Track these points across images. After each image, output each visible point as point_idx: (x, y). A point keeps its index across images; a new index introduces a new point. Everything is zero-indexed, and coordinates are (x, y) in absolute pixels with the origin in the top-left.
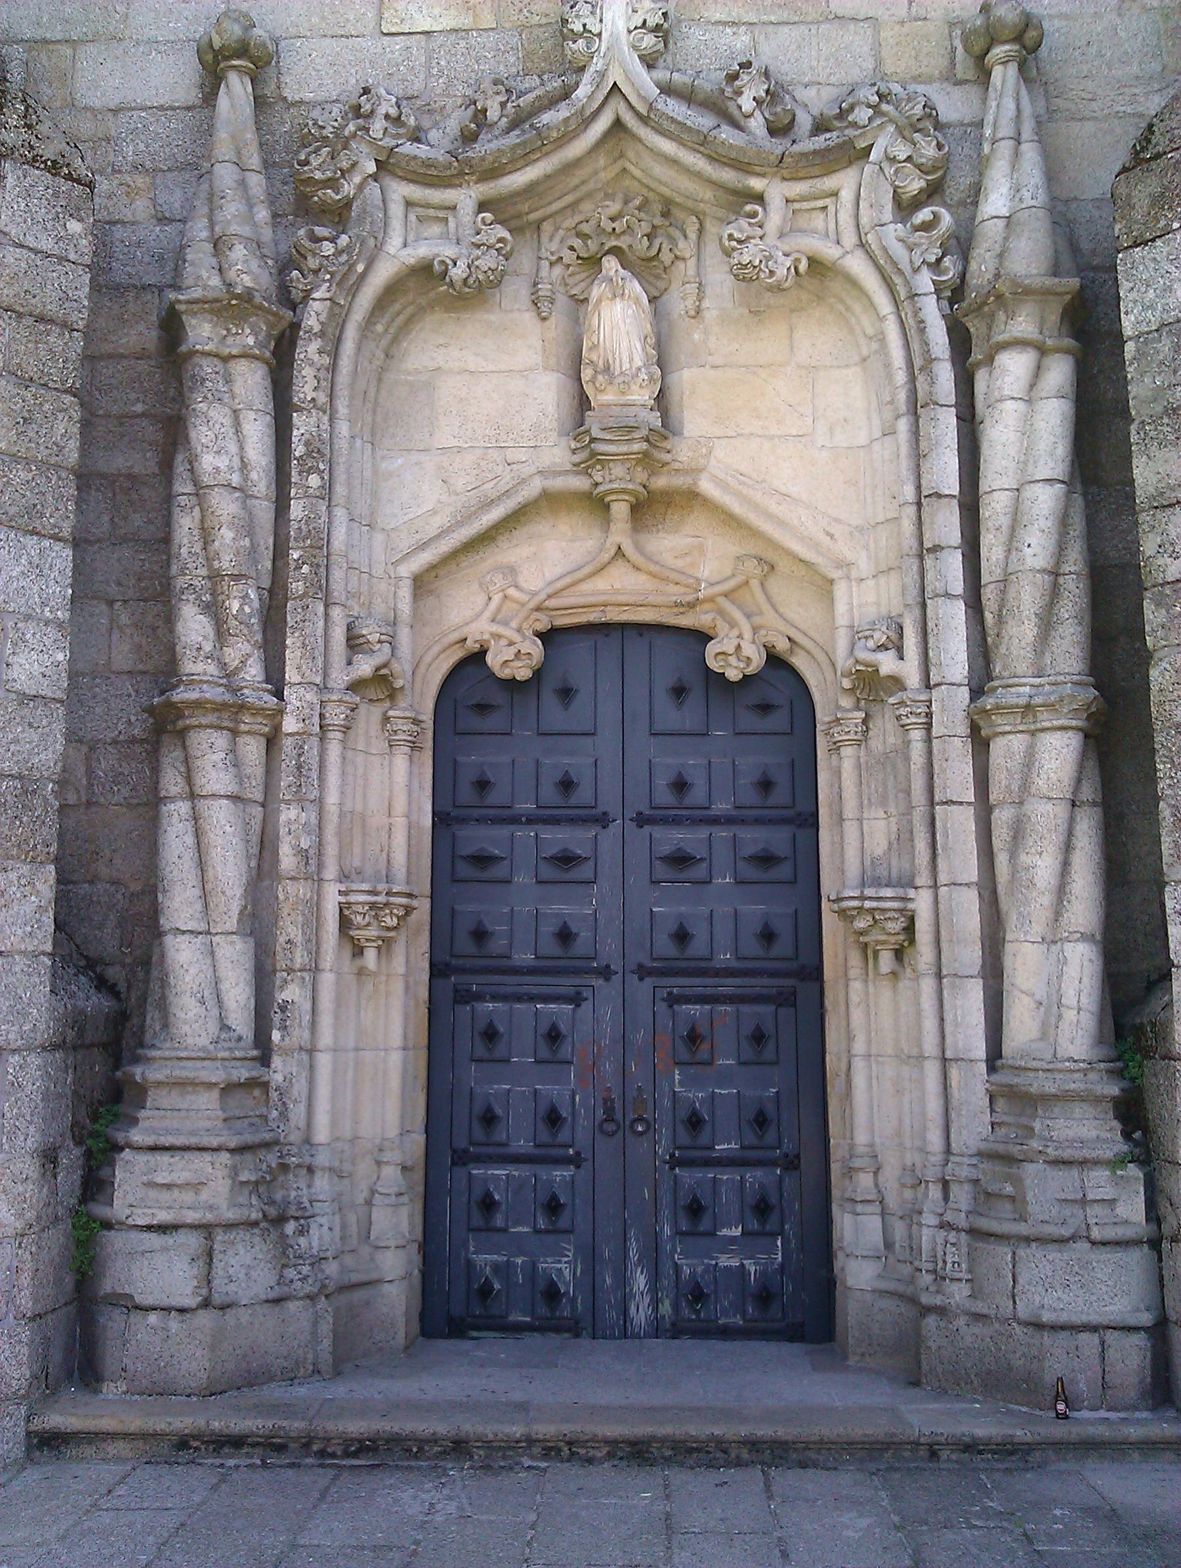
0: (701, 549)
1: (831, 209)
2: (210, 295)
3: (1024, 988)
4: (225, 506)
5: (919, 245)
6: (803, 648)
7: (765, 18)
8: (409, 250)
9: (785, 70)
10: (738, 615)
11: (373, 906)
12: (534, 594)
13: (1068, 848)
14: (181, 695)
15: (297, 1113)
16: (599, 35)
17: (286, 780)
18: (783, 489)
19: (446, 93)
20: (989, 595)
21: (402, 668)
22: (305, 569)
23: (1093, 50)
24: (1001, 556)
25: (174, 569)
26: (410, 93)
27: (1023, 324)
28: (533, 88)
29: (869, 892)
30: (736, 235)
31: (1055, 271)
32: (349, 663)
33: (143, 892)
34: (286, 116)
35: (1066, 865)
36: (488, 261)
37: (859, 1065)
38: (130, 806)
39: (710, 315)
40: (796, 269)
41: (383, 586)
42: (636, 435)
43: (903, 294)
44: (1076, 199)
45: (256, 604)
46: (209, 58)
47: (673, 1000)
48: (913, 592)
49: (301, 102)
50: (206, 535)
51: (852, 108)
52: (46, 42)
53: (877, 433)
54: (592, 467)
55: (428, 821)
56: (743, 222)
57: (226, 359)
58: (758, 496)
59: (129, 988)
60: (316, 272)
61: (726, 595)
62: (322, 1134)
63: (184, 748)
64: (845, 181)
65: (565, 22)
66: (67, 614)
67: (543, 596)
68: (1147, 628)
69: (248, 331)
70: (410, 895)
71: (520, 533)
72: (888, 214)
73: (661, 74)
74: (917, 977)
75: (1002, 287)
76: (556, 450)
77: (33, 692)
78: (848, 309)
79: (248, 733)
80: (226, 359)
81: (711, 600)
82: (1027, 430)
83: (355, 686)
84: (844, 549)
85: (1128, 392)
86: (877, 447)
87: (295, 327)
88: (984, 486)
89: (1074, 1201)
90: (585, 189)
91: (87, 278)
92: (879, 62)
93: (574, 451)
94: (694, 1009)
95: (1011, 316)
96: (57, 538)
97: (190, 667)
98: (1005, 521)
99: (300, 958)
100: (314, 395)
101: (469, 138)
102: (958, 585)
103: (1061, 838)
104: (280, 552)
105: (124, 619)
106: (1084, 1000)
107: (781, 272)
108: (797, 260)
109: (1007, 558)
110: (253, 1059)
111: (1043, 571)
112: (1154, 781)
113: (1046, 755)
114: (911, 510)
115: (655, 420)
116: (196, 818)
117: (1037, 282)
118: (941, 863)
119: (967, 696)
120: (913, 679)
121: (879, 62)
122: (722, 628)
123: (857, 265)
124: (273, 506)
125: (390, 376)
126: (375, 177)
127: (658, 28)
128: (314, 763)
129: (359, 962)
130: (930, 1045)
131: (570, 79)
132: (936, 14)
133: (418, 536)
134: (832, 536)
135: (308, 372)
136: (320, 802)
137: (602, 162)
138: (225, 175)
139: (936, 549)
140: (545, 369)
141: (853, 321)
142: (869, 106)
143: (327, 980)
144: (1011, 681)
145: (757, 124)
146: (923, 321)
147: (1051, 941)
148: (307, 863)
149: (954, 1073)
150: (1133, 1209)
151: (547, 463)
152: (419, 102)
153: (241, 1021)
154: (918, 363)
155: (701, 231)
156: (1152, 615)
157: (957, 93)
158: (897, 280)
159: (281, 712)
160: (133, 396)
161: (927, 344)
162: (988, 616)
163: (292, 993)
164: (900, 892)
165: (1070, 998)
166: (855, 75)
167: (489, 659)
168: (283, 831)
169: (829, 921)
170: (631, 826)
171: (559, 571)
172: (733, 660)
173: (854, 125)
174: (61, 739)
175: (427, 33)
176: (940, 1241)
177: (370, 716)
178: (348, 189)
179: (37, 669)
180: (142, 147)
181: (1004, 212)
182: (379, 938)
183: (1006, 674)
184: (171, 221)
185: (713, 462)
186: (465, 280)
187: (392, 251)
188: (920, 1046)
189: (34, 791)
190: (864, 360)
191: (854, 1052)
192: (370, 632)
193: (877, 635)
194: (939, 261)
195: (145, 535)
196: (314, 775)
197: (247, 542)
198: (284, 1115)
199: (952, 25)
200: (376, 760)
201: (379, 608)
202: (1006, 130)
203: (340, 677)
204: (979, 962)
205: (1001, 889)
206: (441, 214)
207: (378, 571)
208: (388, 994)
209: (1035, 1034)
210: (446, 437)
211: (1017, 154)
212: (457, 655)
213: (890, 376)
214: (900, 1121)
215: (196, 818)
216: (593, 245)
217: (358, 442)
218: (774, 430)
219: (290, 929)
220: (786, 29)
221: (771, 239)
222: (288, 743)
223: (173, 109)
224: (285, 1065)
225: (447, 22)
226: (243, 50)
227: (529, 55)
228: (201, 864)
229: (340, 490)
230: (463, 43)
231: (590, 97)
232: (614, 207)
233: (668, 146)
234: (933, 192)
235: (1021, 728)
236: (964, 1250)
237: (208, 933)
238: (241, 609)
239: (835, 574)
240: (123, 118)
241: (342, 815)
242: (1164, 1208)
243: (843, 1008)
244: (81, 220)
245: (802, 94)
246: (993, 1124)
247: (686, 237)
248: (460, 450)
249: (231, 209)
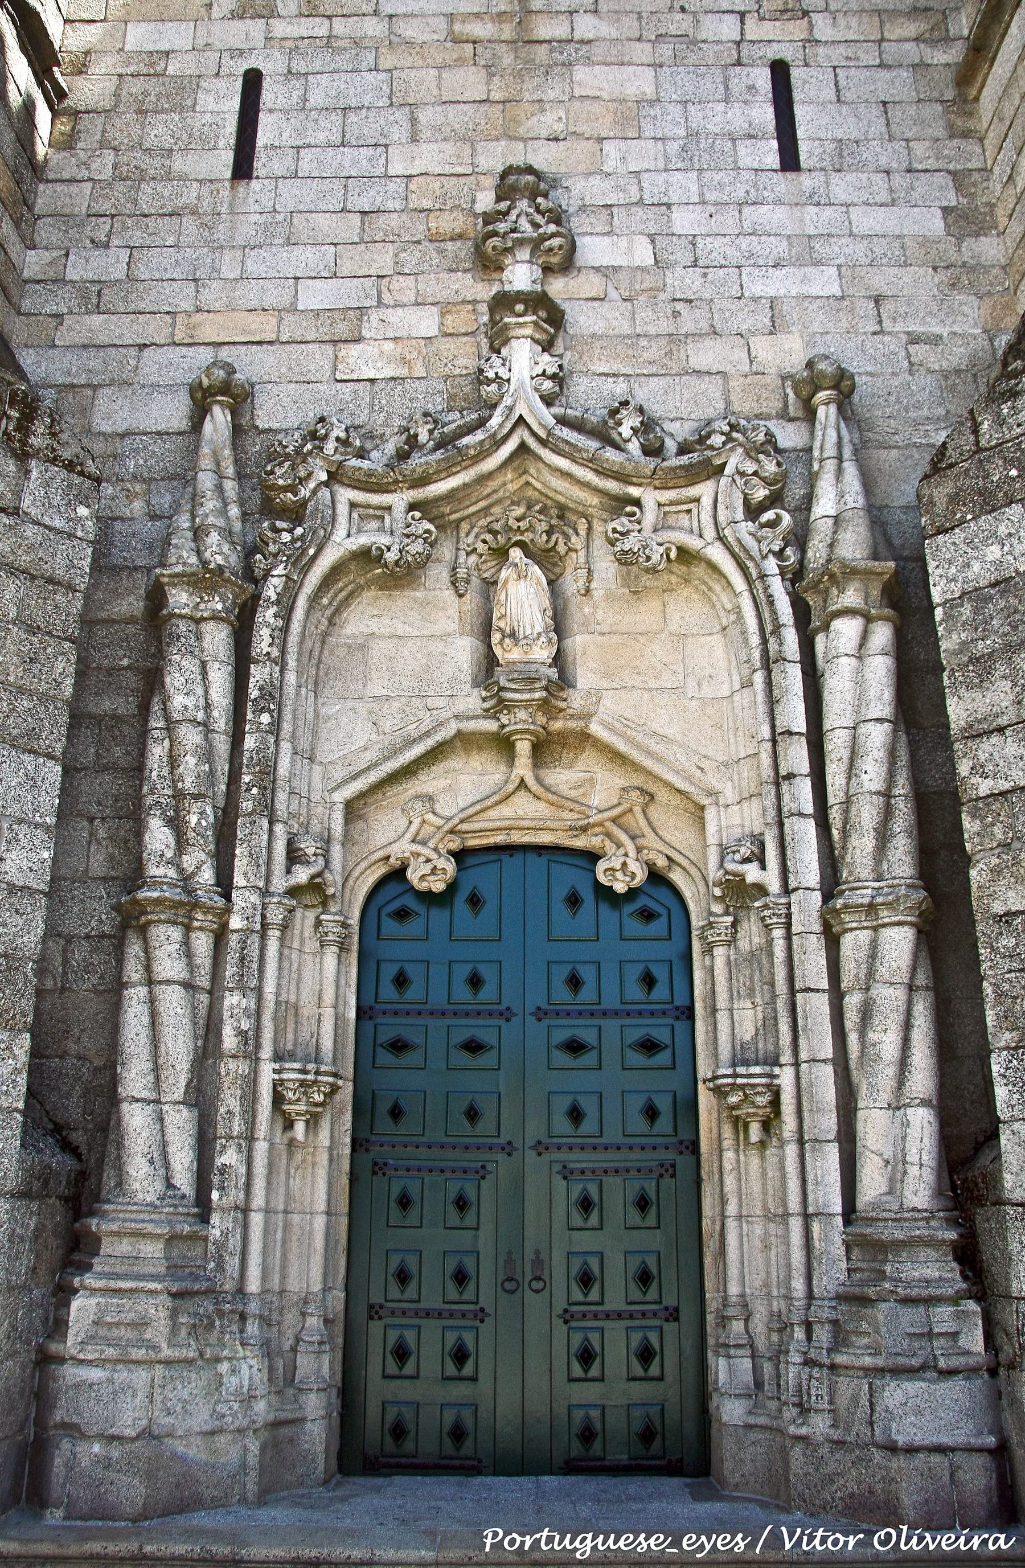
0: (591, 782)
1: (695, 511)
2: (189, 570)
3: (873, 1148)
4: (190, 737)
5: (766, 538)
6: (680, 865)
7: (639, 371)
8: (352, 539)
9: (655, 409)
10: (623, 837)
11: (303, 1083)
12: (449, 819)
13: (907, 1026)
14: (146, 894)
15: (233, 1263)
16: (508, 380)
17: (230, 970)
18: (660, 731)
19: (385, 424)
20: (835, 815)
21: (334, 879)
22: (255, 791)
23: (893, 398)
24: (844, 782)
25: (145, 790)
26: (356, 423)
27: (851, 597)
28: (454, 420)
29: (741, 1070)
30: (619, 529)
31: (875, 556)
32: (288, 871)
33: (105, 1067)
34: (257, 440)
35: (906, 1042)
36: (417, 547)
37: (731, 1224)
38: (96, 992)
39: (598, 594)
40: (668, 555)
41: (320, 810)
42: (537, 685)
43: (754, 574)
44: (887, 506)
45: (211, 819)
46: (199, 395)
48: (772, 813)
49: (270, 430)
50: (173, 761)
51: (709, 436)
52: (73, 386)
53: (737, 686)
54: (501, 711)
55: (352, 1014)
56: (624, 520)
57: (198, 621)
58: (640, 738)
59: (89, 1151)
60: (276, 555)
61: (614, 820)
62: (253, 1286)
63: (145, 940)
64: (705, 490)
65: (481, 371)
66: (54, 820)
67: (456, 820)
68: (966, 836)
69: (217, 599)
70: (335, 1075)
71: (438, 769)
72: (740, 515)
73: (557, 410)
74: (782, 1144)
75: (835, 568)
76: (468, 699)
77: (21, 884)
78: (710, 589)
79: (200, 929)
80: (198, 621)
81: (601, 824)
82: (859, 680)
83: (293, 892)
84: (713, 780)
85: (939, 647)
86: (737, 697)
87: (256, 597)
88: (827, 725)
89: (922, 1335)
90: (495, 496)
91: (89, 551)
92: (728, 403)
93: (484, 700)
95: (842, 591)
96: (50, 756)
97: (153, 870)
98: (846, 754)
99: (237, 1126)
100: (269, 649)
101: (402, 456)
102: (809, 808)
103: (902, 1018)
104: (234, 777)
105: (102, 833)
106: (925, 1157)
107: (655, 558)
108: (668, 549)
109: (848, 783)
110: (194, 1215)
111: (878, 793)
112: (978, 963)
113: (887, 947)
114: (768, 745)
115: (553, 673)
116: (152, 1001)
117: (862, 564)
118: (802, 1042)
119: (820, 898)
120: (774, 886)
121: (728, 403)
122: (610, 847)
123: (717, 554)
124: (230, 740)
125: (332, 639)
126: (326, 484)
127: (553, 377)
128: (255, 954)
129: (289, 1134)
130: (794, 1204)
131: (485, 413)
132: (773, 371)
133: (351, 768)
134: (702, 770)
135: (265, 632)
136: (259, 991)
137: (509, 476)
138: (206, 481)
139: (790, 776)
140: (461, 634)
141: (714, 598)
142: (722, 434)
143: (261, 1148)
144: (856, 885)
145: (634, 447)
146: (771, 596)
147: (896, 1106)
148: (246, 1043)
149: (816, 1227)
150: (975, 1341)
151: (462, 709)
152: (363, 431)
153: (184, 1181)
154: (769, 628)
155: (590, 529)
156: (969, 825)
157: (790, 427)
158: (750, 564)
159: (228, 911)
160: (121, 653)
161: (776, 613)
162: (835, 833)
163: (229, 1157)
164: (768, 1069)
165: (912, 1157)
166: (711, 413)
167: (409, 874)
168: (226, 1015)
169: (705, 1099)
170: (531, 1020)
171: (471, 799)
172: (619, 875)
173: (712, 448)
174: (42, 925)
175: (372, 381)
176: (804, 1376)
177: (305, 920)
178: (304, 492)
179: (25, 864)
180: (141, 462)
181: (833, 513)
182: (307, 1112)
183: (851, 879)
184: (160, 518)
185: (602, 709)
186: (397, 563)
187: (338, 540)
188: (785, 1205)
189: (17, 968)
190: (724, 629)
191: (727, 1214)
192: (308, 847)
193: (743, 850)
194: (782, 550)
195: (122, 763)
196: (255, 966)
197: (207, 767)
198: (220, 1267)
199: (784, 378)
200: (309, 958)
201: (316, 827)
202: (830, 451)
203: (280, 883)
204: (835, 1127)
205: (853, 1065)
206: (379, 513)
207: (316, 797)
208: (314, 1164)
209: (884, 1189)
210: (376, 688)
211: (839, 471)
212: (381, 871)
213: (746, 641)
214: (768, 1273)
215: (152, 1001)
216: (501, 539)
217: (304, 690)
218: (652, 684)
219: (230, 1101)
220: (655, 379)
221: (647, 532)
222: (233, 940)
223: (168, 434)
224: (222, 1222)
225: (389, 372)
226: (226, 388)
227: (452, 397)
228: (155, 1042)
229: (287, 727)
230: (400, 388)
231: (501, 425)
232: (519, 511)
233: (563, 463)
234: (775, 500)
235: (865, 924)
236: (826, 1383)
237: (158, 1102)
238: (199, 823)
239: (705, 801)
240: (128, 440)
241: (278, 1003)
242: (1001, 1338)
243: (717, 1177)
244: (88, 507)
245: (668, 426)
246: (849, 1270)
247: (577, 534)
248: (388, 698)
249: (210, 504)
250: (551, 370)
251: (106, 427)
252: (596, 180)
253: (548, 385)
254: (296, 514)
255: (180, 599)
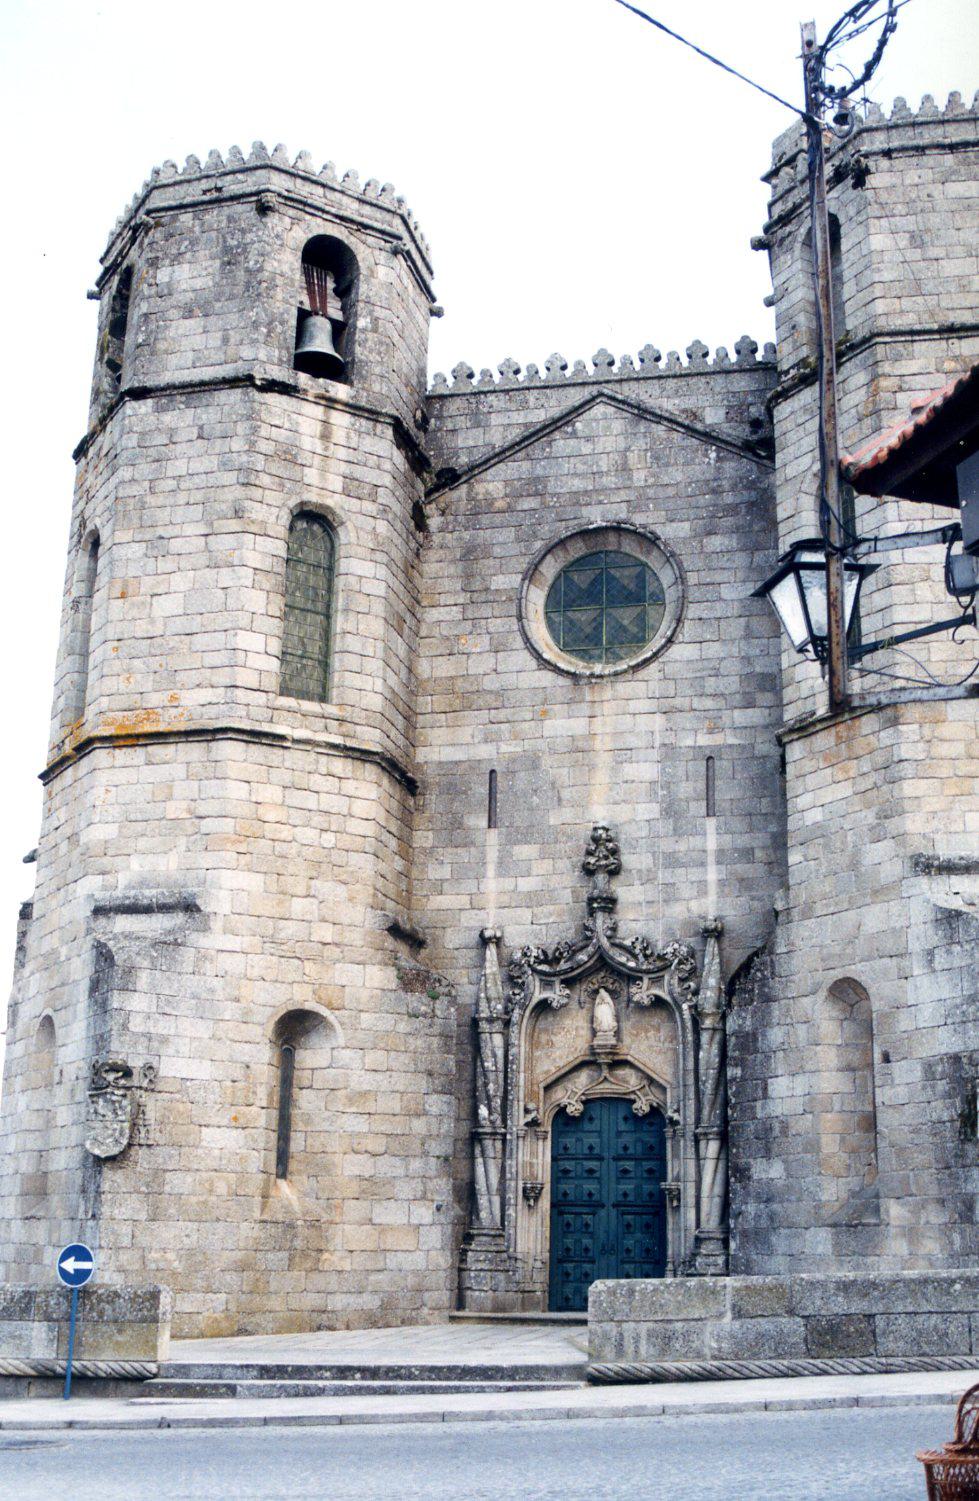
13: (715, 1171)
36: (565, 1001)
47: (623, 1214)
50: (486, 1085)
81: (633, 1092)
83: (527, 1124)
94: (629, 1217)
99: (512, 1201)
143: (519, 1207)
167: (568, 1110)
203: (522, 1121)
219: (510, 1195)
250: (611, 926)
251: (451, 946)
252: (634, 826)
253: (609, 933)
254: (522, 986)
255: (484, 1026)
